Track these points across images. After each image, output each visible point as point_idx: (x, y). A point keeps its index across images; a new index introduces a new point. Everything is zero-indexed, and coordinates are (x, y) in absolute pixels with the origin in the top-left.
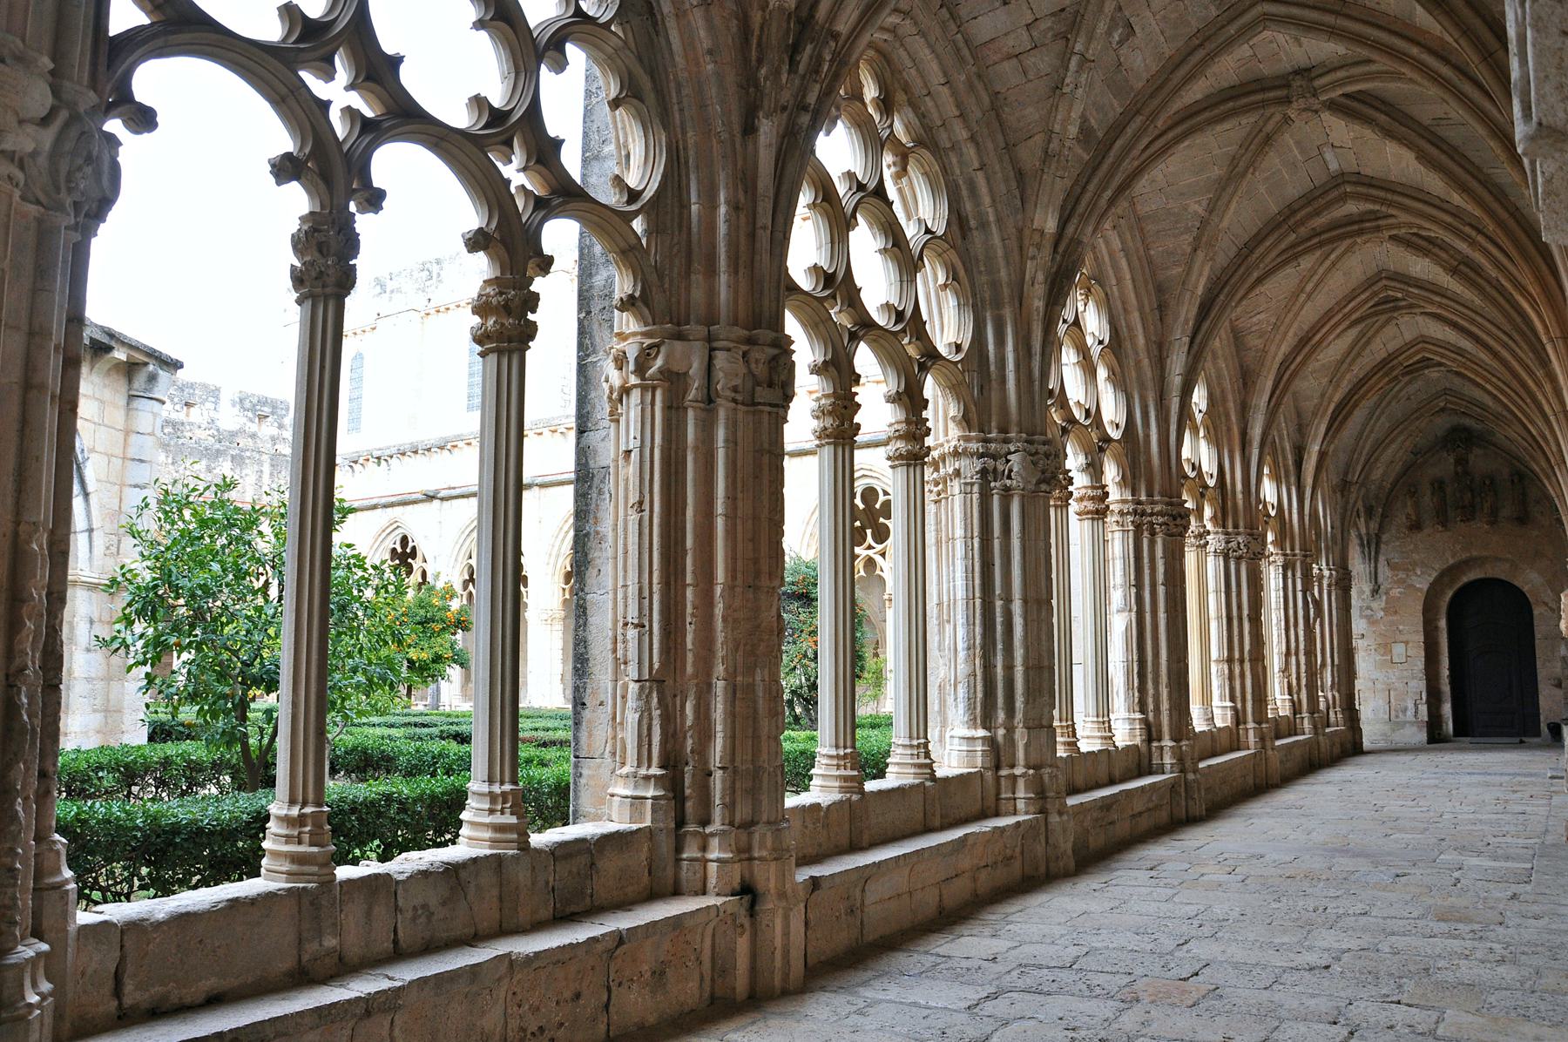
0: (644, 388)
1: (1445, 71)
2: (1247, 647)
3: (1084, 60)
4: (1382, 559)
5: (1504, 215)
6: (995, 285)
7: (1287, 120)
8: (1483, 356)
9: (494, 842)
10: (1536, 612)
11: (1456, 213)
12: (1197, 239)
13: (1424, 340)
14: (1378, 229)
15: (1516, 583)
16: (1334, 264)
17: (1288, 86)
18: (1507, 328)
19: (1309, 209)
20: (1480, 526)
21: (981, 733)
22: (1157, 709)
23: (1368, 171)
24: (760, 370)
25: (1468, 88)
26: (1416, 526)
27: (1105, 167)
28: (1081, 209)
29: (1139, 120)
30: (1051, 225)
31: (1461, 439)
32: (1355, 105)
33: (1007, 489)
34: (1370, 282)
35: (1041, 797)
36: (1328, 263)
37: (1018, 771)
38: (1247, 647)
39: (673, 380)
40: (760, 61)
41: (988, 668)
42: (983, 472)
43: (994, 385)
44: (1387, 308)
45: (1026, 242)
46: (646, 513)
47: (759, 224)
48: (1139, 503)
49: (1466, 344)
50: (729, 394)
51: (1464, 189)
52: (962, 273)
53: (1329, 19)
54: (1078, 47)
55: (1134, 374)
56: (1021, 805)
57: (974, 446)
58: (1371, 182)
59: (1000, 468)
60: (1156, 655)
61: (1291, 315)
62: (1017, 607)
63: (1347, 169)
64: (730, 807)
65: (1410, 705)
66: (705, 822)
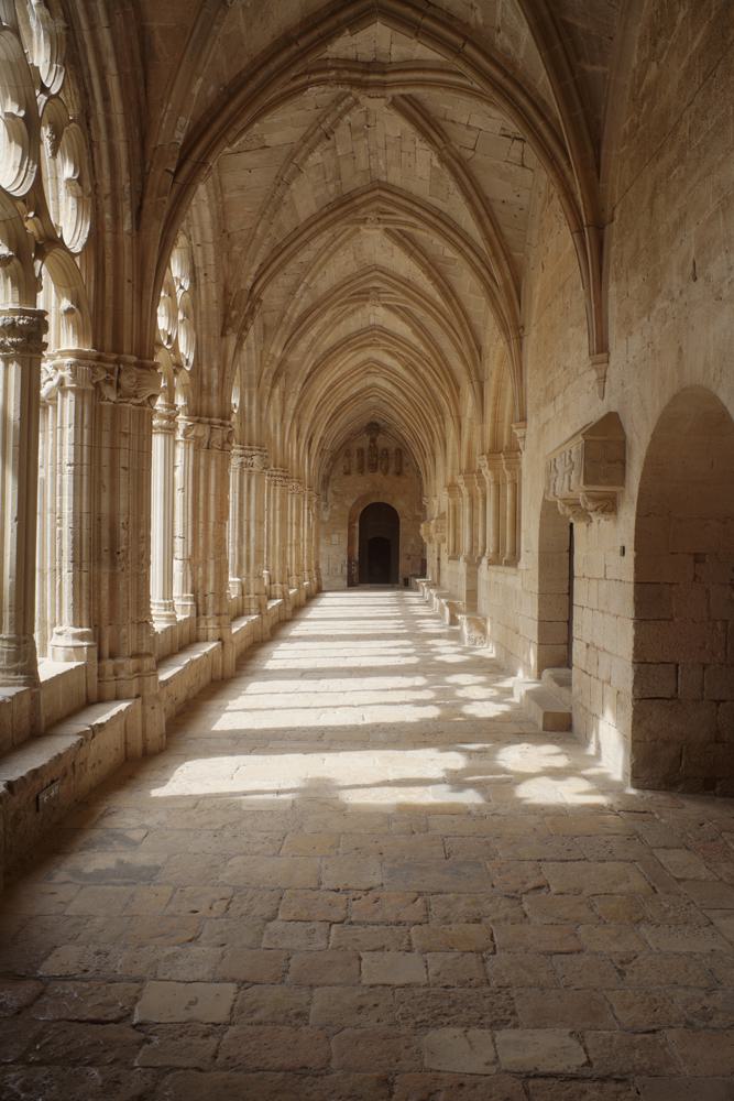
0: (185, 442)
1: (443, 320)
2: (294, 538)
3: (307, 287)
4: (330, 489)
8: (401, 397)
9: (167, 622)
10: (401, 521)
13: (374, 386)
18: (424, 396)
20: (379, 474)
21: (237, 579)
22: (274, 569)
25: (451, 330)
26: (347, 473)
28: (288, 346)
29: (318, 310)
31: (374, 428)
35: (261, 608)
37: (252, 596)
38: (294, 538)
40: (233, 308)
41: (240, 550)
47: (226, 375)
49: (395, 391)
51: (428, 348)
53: (403, 287)
54: (306, 281)
56: (252, 610)
58: (386, 331)
60: (274, 543)
62: (252, 524)
64: (214, 607)
65: (339, 567)
66: (205, 614)
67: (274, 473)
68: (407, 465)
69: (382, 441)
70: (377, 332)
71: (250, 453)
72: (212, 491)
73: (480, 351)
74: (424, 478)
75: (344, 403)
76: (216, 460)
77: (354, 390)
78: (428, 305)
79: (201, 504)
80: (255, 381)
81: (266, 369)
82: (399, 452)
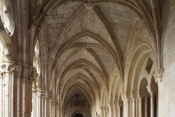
1: (110, 49)
4: (67, 110)
5: (103, 69)
6: (44, 65)
7: (81, 49)
11: (97, 67)
12: (64, 64)
13: (79, 82)
14: (83, 67)
15: (82, 114)
16: (75, 71)
17: (83, 45)
19: (78, 63)
20: (79, 107)
23: (86, 59)
24: (30, 73)
26: (71, 106)
27: (62, 50)
28: (58, 56)
30: (54, 57)
31: (77, 96)
32: (90, 50)
33: (44, 98)
34: (79, 73)
36: (75, 70)
39: (15, 72)
42: (41, 95)
43: (43, 81)
44: (79, 77)
45: (49, 59)
46: (10, 97)
48: (51, 101)
50: (26, 77)
52: (40, 62)
53: (96, 37)
55: (52, 82)
57: (40, 91)
58: (86, 61)
59: (44, 94)
61: (68, 77)
63: (84, 58)
67: (53, 102)
68: (85, 104)
69: (79, 99)
70: (83, 61)
71: (44, 91)
72: (24, 97)
73: (123, 58)
74: (90, 106)
75: (71, 87)
76: (26, 84)
77: (74, 83)
78: (104, 43)
79: (18, 103)
80: (46, 66)
81: (50, 63)
82: (84, 101)
